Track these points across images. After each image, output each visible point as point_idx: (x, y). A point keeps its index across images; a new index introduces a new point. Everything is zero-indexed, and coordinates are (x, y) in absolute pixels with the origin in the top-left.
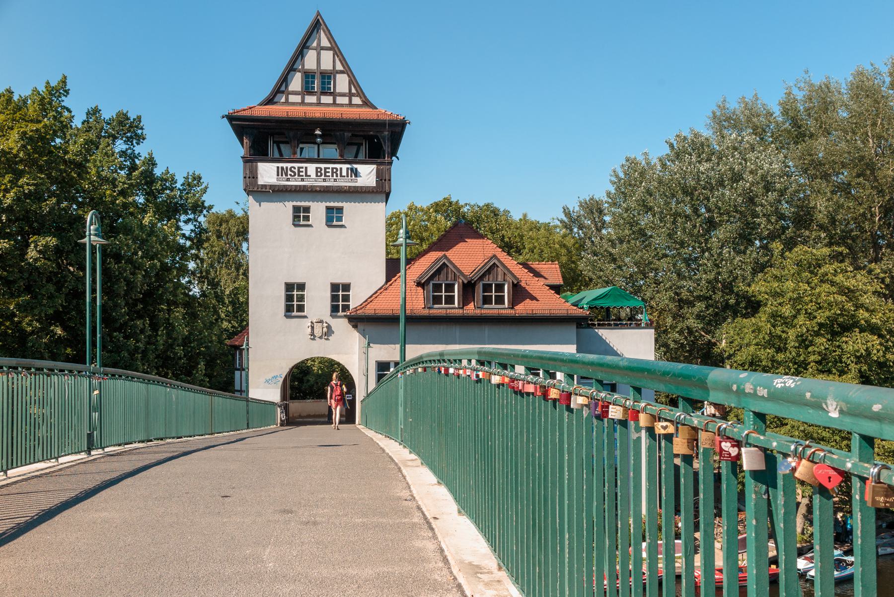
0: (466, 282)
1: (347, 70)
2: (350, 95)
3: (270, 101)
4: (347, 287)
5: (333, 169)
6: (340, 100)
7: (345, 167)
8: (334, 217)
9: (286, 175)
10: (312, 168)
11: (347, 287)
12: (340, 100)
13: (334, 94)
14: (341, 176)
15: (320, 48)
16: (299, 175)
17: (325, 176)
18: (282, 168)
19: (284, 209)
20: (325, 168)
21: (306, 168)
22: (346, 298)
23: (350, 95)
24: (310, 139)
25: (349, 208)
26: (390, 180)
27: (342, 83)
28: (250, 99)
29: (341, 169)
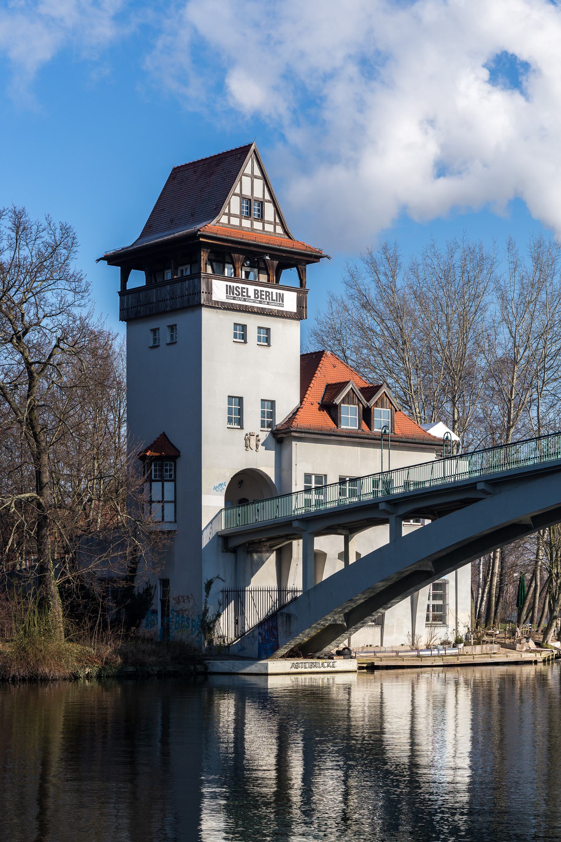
0: (366, 407)
4: (273, 403)
5: (266, 292)
9: (233, 294)
10: (251, 289)
11: (273, 403)
14: (272, 300)
16: (242, 295)
17: (261, 298)
18: (230, 286)
20: (261, 291)
21: (247, 289)
22: (272, 415)
23: (275, 224)
26: (306, 308)
29: (272, 292)
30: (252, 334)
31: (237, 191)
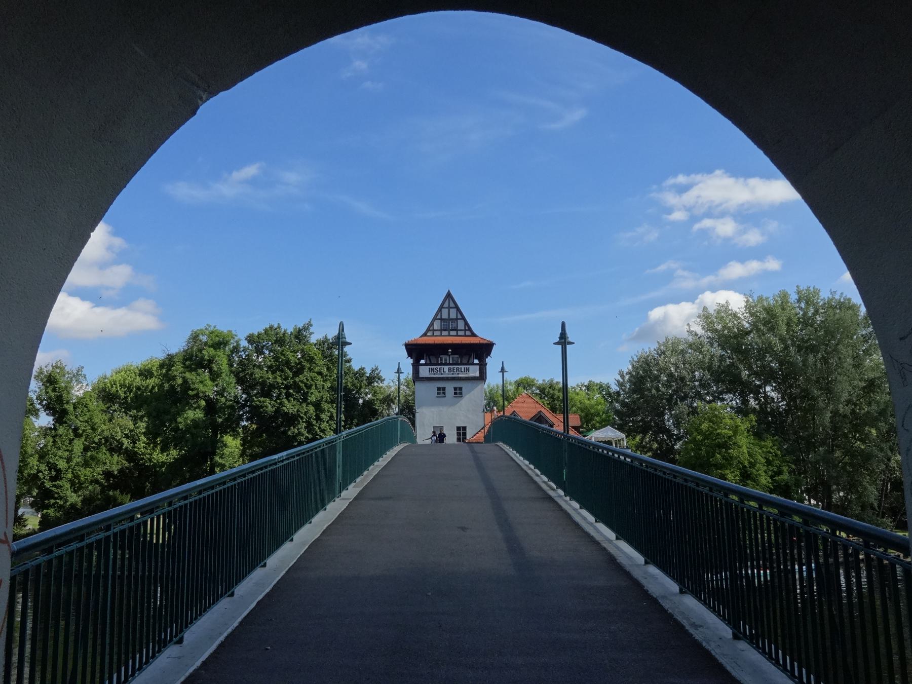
1: (463, 318)
2: (465, 330)
3: (425, 335)
4: (464, 428)
6: (460, 333)
7: (463, 367)
8: (458, 392)
10: (446, 368)
11: (464, 428)
12: (460, 333)
13: (456, 330)
15: (449, 308)
19: (433, 387)
22: (465, 434)
23: (465, 330)
24: (446, 353)
25: (465, 386)
27: (461, 325)
28: (415, 334)
30: (450, 391)
31: (439, 317)
